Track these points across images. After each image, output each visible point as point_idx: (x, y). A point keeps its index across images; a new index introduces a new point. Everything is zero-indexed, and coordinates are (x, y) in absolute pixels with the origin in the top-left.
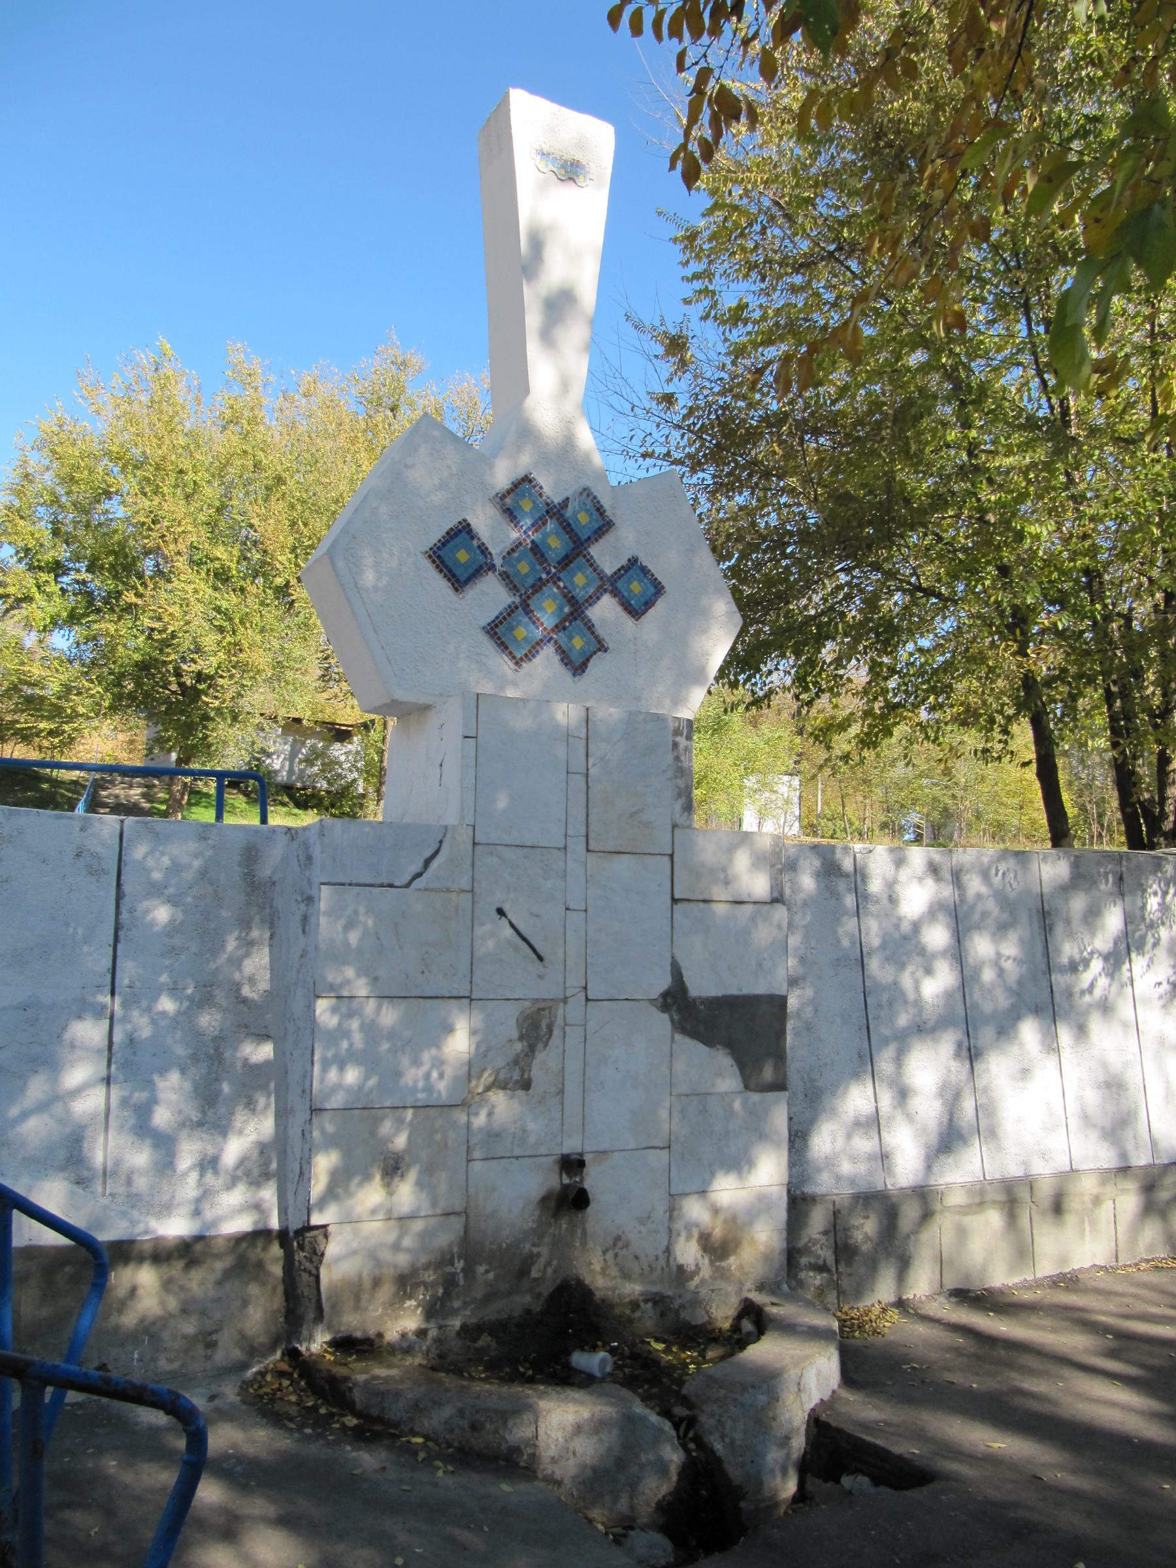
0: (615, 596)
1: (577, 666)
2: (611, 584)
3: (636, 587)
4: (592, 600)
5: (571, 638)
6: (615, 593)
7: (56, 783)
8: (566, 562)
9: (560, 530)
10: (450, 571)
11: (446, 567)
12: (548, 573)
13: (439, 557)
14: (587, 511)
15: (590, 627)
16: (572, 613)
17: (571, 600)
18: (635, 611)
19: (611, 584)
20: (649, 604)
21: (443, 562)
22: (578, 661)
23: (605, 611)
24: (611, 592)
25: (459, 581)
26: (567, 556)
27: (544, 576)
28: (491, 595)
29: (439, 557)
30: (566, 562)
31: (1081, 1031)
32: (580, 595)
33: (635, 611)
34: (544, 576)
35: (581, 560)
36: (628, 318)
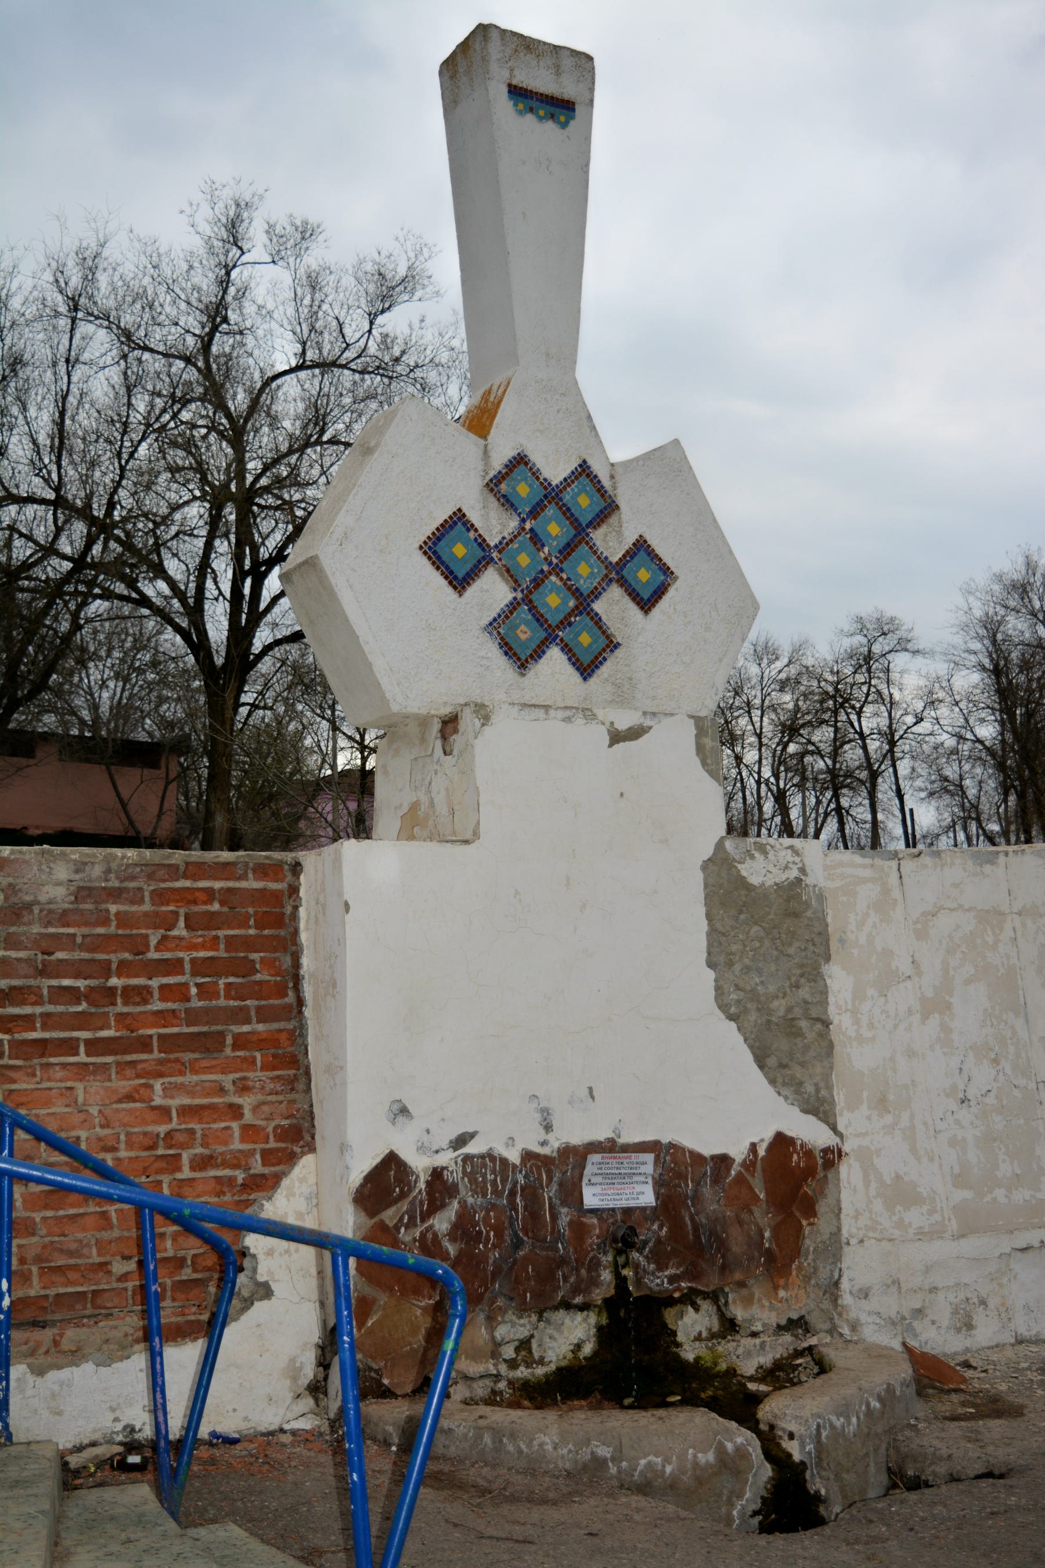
0: (622, 586)
1: (586, 669)
2: (617, 573)
3: (644, 575)
4: (595, 594)
5: (578, 634)
6: (623, 582)
7: (223, 689)
8: (567, 550)
9: (561, 516)
10: (447, 567)
11: (443, 563)
12: (550, 564)
13: (433, 549)
14: (586, 492)
15: (597, 620)
16: (577, 607)
17: (576, 593)
18: (646, 603)
19: (617, 573)
20: (660, 592)
21: (439, 558)
22: (586, 660)
23: (613, 606)
24: (618, 581)
25: (459, 582)
26: (568, 544)
27: (546, 568)
28: (493, 591)
29: (433, 549)
30: (567, 550)
31: (942, 866)
32: (585, 586)
33: (646, 603)
34: (546, 568)
35: (584, 548)
36: (447, 1521)
